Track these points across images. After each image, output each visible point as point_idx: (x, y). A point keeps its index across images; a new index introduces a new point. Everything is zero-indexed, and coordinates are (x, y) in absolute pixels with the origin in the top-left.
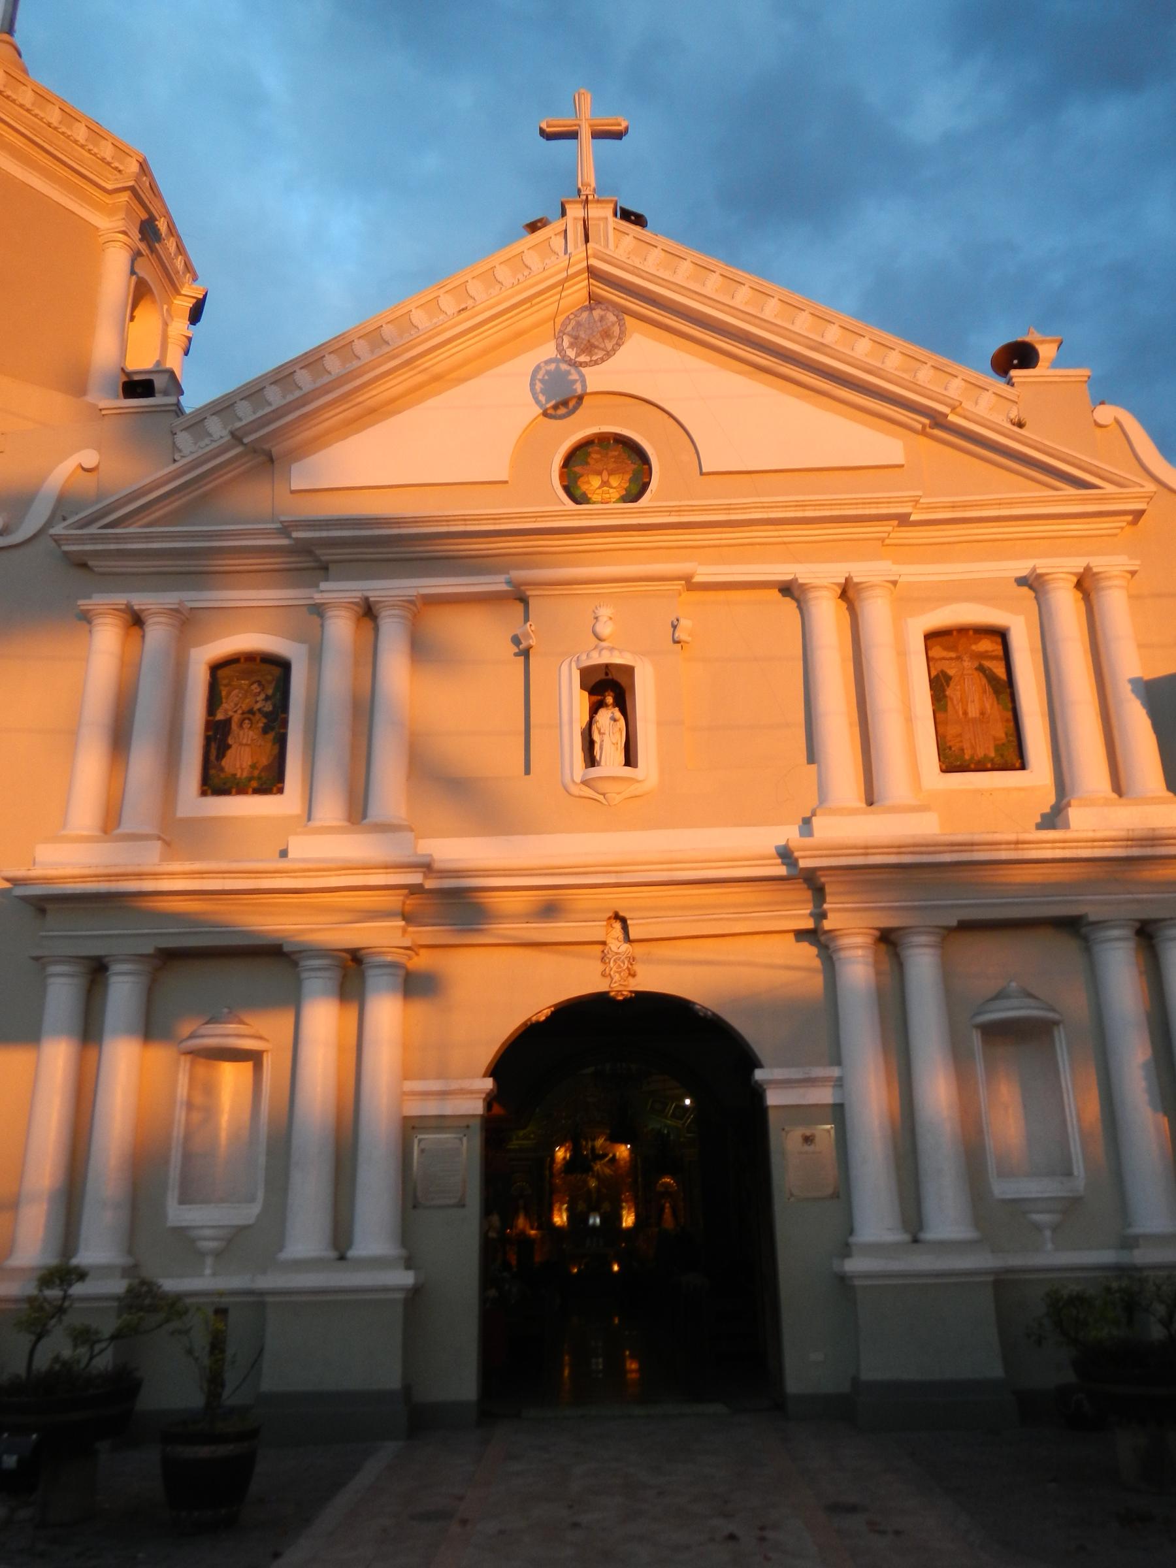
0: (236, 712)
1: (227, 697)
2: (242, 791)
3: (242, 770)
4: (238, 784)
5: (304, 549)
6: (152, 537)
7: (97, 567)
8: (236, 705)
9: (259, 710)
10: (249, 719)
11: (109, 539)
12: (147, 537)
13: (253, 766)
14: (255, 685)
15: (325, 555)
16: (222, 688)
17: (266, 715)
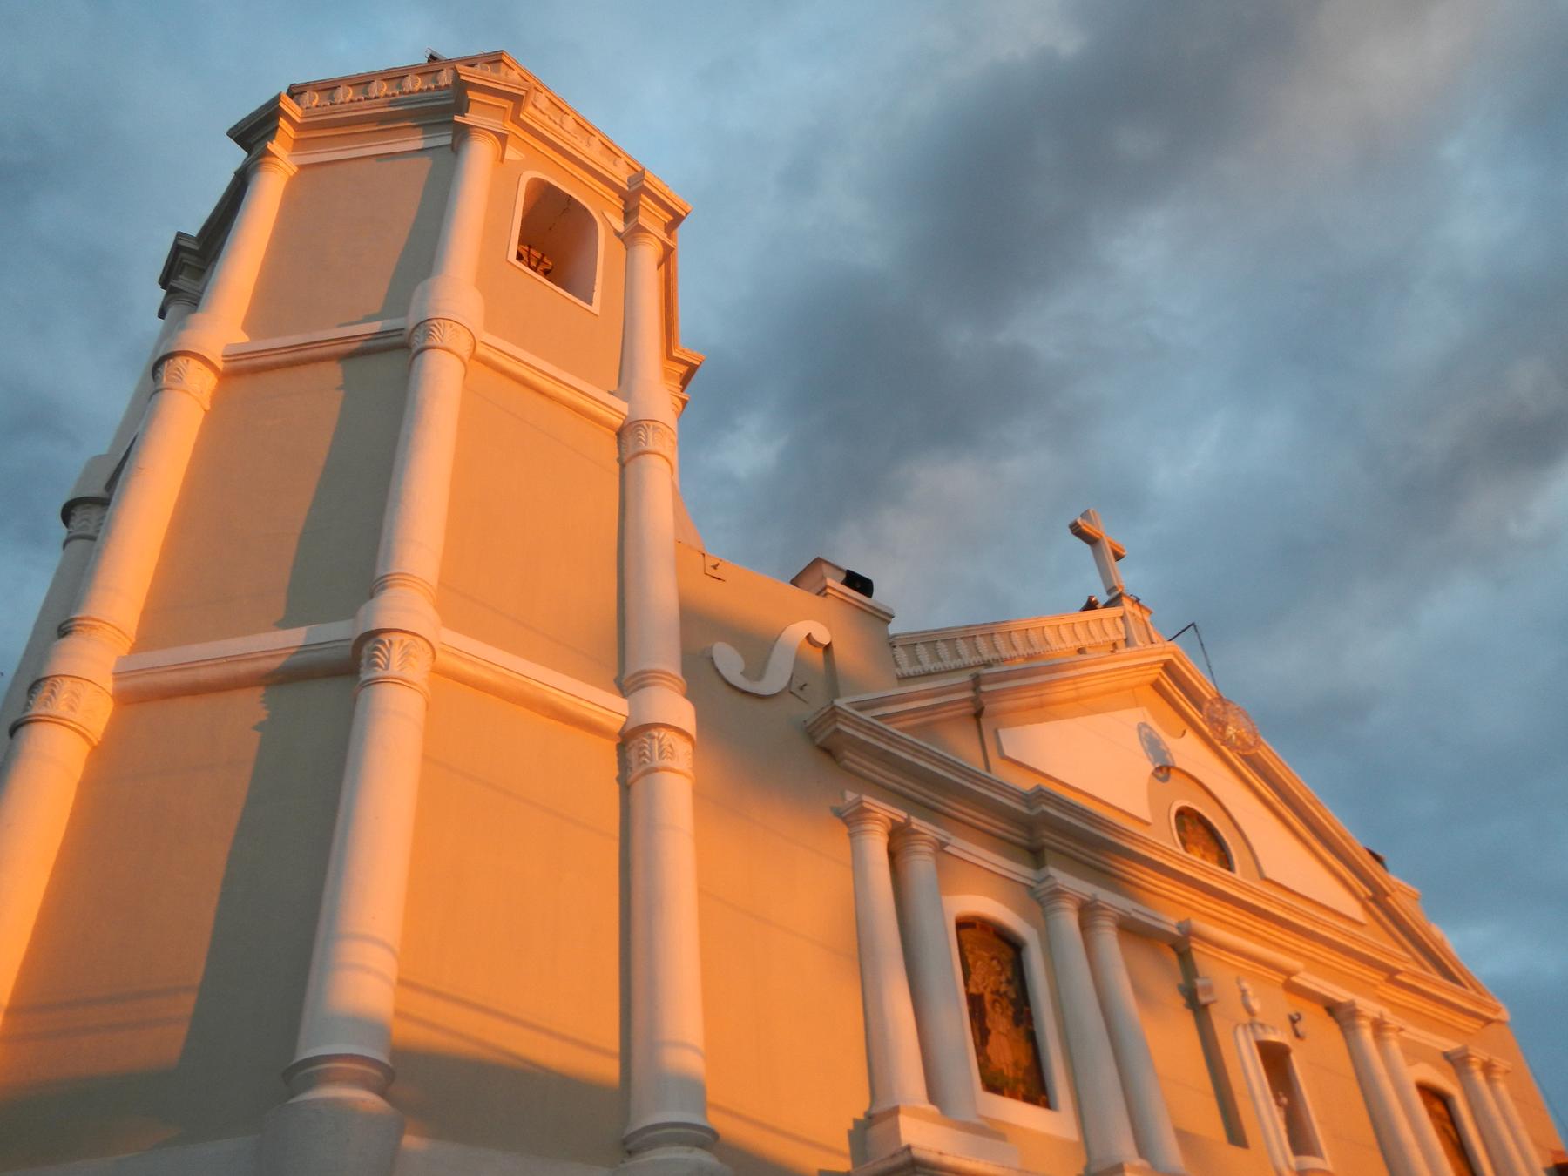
0: (985, 988)
1: (976, 962)
2: (1013, 1095)
3: (1007, 1066)
4: (1007, 1083)
5: (1029, 825)
6: (920, 752)
7: (853, 761)
8: (984, 980)
9: (1005, 993)
10: (1001, 1004)
11: (882, 735)
12: (916, 751)
13: (1016, 1064)
14: (995, 963)
15: (1048, 838)
16: (967, 954)
17: (1013, 1003)
